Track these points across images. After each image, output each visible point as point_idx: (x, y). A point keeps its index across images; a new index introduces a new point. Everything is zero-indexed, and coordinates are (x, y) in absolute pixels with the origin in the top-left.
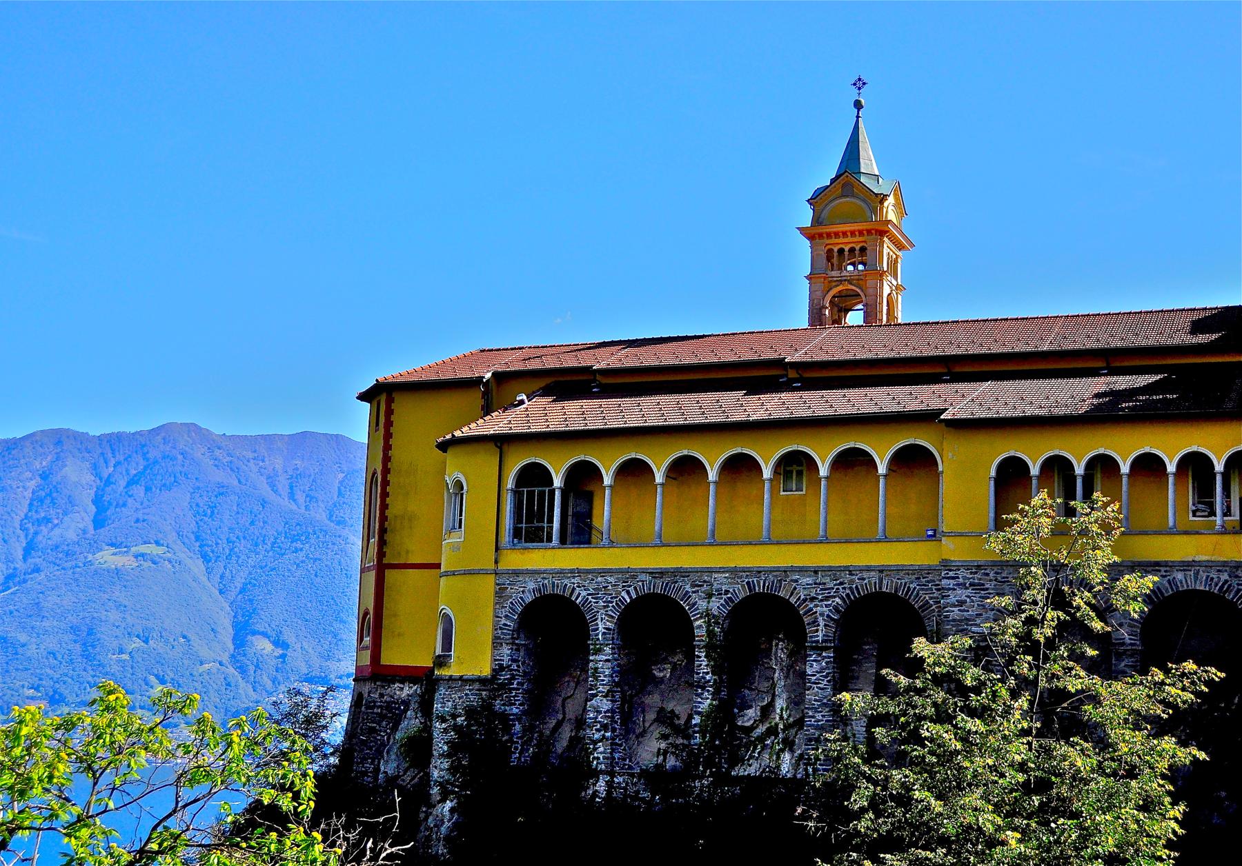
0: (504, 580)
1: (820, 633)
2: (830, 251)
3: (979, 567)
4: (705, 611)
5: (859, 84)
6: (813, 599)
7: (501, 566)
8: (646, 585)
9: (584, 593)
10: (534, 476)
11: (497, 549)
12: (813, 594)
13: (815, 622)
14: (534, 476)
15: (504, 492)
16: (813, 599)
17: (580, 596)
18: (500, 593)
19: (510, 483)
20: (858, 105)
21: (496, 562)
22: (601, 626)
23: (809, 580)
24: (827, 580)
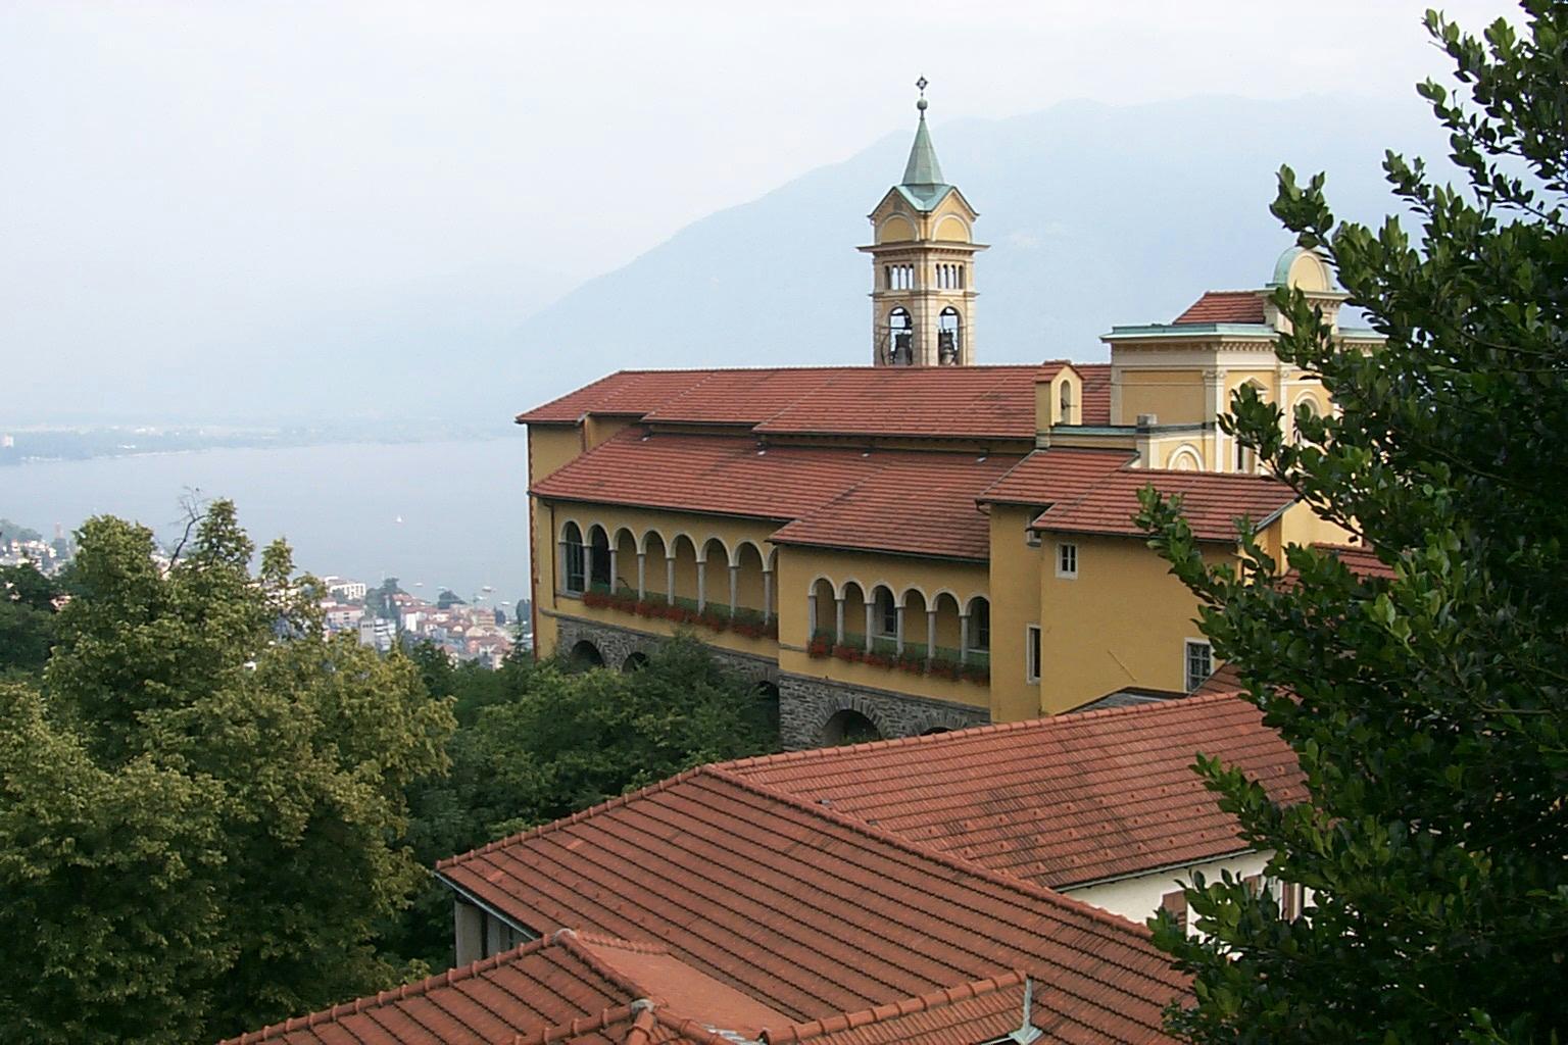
2: (887, 268)
3: (803, 681)
5: (922, 83)
7: (559, 612)
8: (637, 645)
10: (572, 530)
11: (555, 595)
14: (572, 530)
15: (557, 546)
17: (601, 645)
18: (560, 632)
19: (560, 538)
20: (922, 107)
21: (556, 607)
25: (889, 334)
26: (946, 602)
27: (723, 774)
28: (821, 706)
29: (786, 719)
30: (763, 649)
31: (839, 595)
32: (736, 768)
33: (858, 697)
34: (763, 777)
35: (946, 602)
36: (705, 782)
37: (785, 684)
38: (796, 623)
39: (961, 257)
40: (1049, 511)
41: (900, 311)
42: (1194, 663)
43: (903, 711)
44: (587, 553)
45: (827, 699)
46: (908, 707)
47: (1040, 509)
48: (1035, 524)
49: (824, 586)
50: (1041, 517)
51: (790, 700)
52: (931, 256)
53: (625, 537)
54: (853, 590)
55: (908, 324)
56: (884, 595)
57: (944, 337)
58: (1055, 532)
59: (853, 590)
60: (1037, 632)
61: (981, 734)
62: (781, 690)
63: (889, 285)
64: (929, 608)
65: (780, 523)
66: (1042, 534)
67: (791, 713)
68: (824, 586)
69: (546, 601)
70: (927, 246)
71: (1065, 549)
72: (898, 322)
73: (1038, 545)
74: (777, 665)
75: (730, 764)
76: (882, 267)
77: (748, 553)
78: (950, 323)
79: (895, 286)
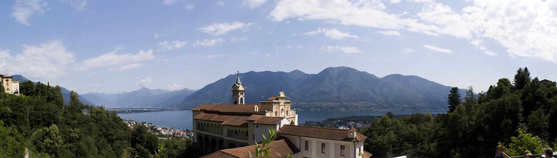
0: (197, 133)
4: (210, 139)
26: (243, 131)
35: (243, 131)
49: (229, 130)
56: (236, 130)
59: (232, 130)
68: (229, 130)
69: (195, 130)
77: (219, 125)
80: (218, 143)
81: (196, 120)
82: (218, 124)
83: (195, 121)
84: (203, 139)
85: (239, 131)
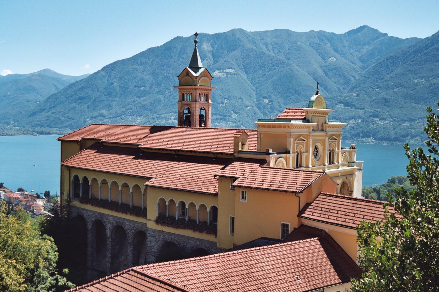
1: (130, 240)
2: (183, 94)
6: (129, 229)
9: (86, 216)
10: (76, 178)
12: (129, 228)
13: (129, 236)
16: (129, 229)
17: (85, 216)
19: (72, 180)
20: (196, 42)
22: (89, 227)
23: (127, 223)
24: (131, 224)
25: (183, 115)
27: (138, 270)
28: (161, 239)
29: (149, 244)
30: (141, 220)
31: (167, 204)
32: (142, 268)
33: (173, 237)
34: (152, 271)
35: (203, 206)
36: (132, 273)
37: (149, 232)
38: (153, 213)
39: (207, 91)
40: (238, 180)
41: (187, 108)
42: (283, 230)
43: (188, 242)
44: (81, 186)
45: (162, 237)
46: (190, 241)
47: (235, 179)
48: (234, 184)
49: (162, 201)
50: (236, 182)
51: (150, 238)
52: (197, 91)
53: (94, 180)
54: (172, 201)
55: (189, 112)
56: (183, 204)
57: (201, 117)
58: (240, 187)
60: (233, 219)
61: (220, 256)
62: (147, 234)
63: (183, 99)
64: (197, 209)
65: (149, 178)
66: (236, 188)
67: (151, 241)
68: (162, 201)
70: (197, 87)
71: (243, 192)
72: (186, 111)
73: (234, 190)
74: (146, 225)
75: (140, 267)
76: (181, 95)
77: (136, 187)
78: (203, 112)
79: (185, 100)
80: (130, 240)
81: (69, 168)
82: (131, 184)
83: (66, 173)
84: (90, 227)
85: (192, 205)
